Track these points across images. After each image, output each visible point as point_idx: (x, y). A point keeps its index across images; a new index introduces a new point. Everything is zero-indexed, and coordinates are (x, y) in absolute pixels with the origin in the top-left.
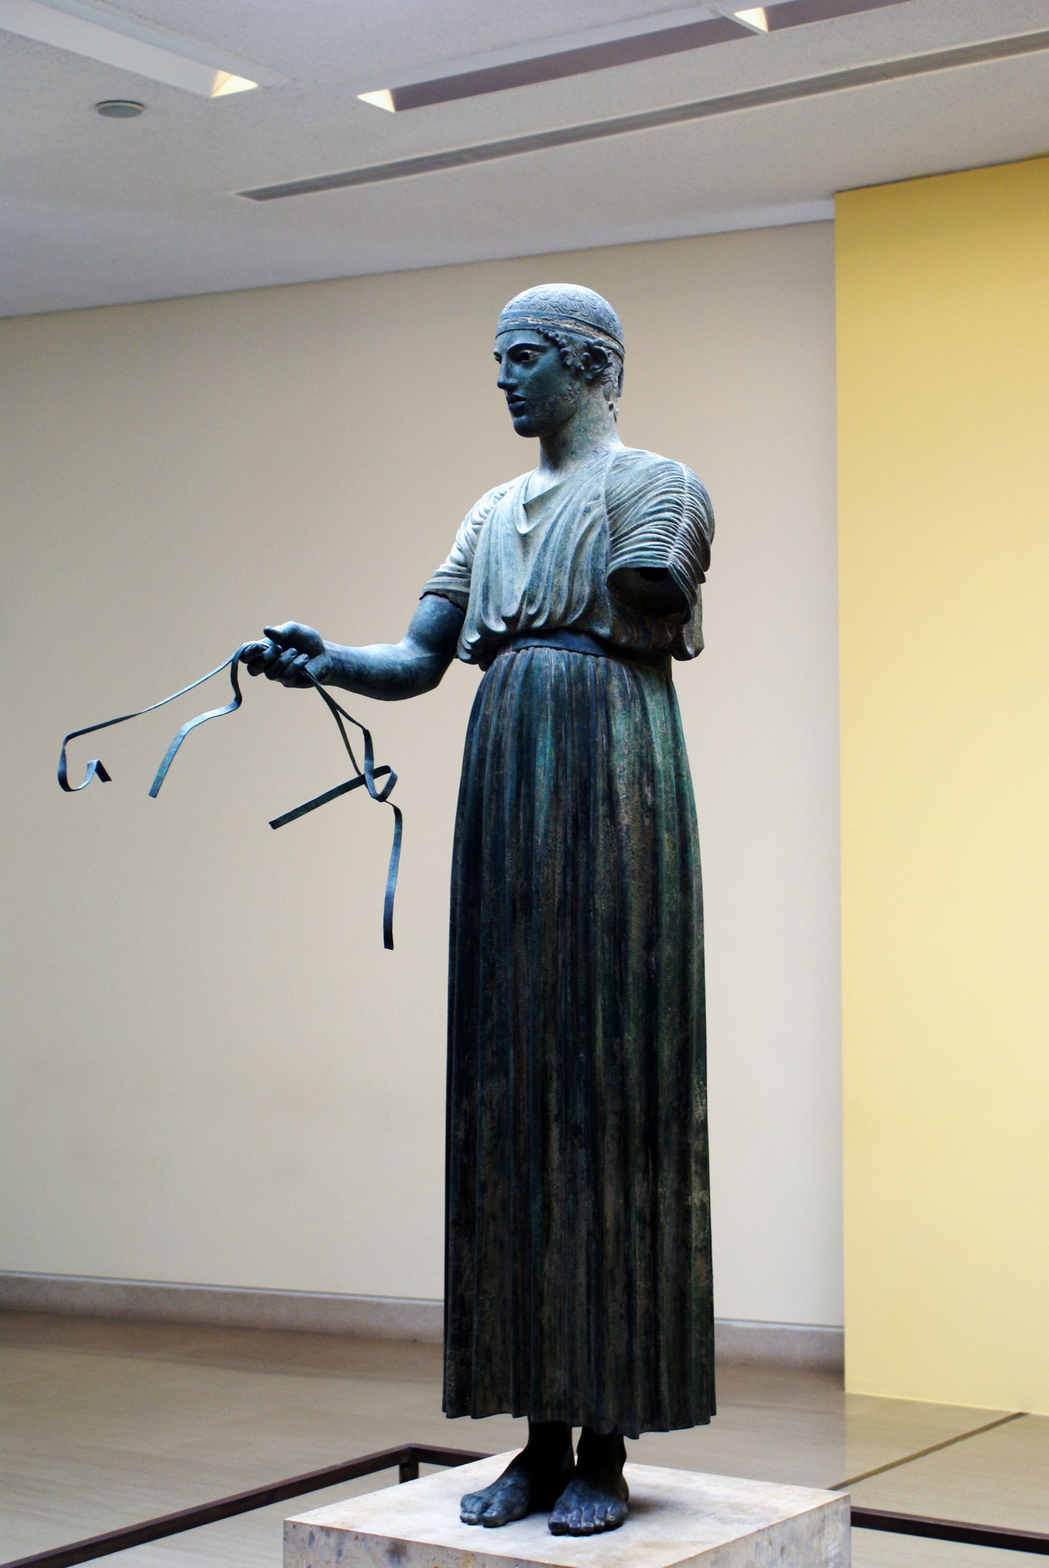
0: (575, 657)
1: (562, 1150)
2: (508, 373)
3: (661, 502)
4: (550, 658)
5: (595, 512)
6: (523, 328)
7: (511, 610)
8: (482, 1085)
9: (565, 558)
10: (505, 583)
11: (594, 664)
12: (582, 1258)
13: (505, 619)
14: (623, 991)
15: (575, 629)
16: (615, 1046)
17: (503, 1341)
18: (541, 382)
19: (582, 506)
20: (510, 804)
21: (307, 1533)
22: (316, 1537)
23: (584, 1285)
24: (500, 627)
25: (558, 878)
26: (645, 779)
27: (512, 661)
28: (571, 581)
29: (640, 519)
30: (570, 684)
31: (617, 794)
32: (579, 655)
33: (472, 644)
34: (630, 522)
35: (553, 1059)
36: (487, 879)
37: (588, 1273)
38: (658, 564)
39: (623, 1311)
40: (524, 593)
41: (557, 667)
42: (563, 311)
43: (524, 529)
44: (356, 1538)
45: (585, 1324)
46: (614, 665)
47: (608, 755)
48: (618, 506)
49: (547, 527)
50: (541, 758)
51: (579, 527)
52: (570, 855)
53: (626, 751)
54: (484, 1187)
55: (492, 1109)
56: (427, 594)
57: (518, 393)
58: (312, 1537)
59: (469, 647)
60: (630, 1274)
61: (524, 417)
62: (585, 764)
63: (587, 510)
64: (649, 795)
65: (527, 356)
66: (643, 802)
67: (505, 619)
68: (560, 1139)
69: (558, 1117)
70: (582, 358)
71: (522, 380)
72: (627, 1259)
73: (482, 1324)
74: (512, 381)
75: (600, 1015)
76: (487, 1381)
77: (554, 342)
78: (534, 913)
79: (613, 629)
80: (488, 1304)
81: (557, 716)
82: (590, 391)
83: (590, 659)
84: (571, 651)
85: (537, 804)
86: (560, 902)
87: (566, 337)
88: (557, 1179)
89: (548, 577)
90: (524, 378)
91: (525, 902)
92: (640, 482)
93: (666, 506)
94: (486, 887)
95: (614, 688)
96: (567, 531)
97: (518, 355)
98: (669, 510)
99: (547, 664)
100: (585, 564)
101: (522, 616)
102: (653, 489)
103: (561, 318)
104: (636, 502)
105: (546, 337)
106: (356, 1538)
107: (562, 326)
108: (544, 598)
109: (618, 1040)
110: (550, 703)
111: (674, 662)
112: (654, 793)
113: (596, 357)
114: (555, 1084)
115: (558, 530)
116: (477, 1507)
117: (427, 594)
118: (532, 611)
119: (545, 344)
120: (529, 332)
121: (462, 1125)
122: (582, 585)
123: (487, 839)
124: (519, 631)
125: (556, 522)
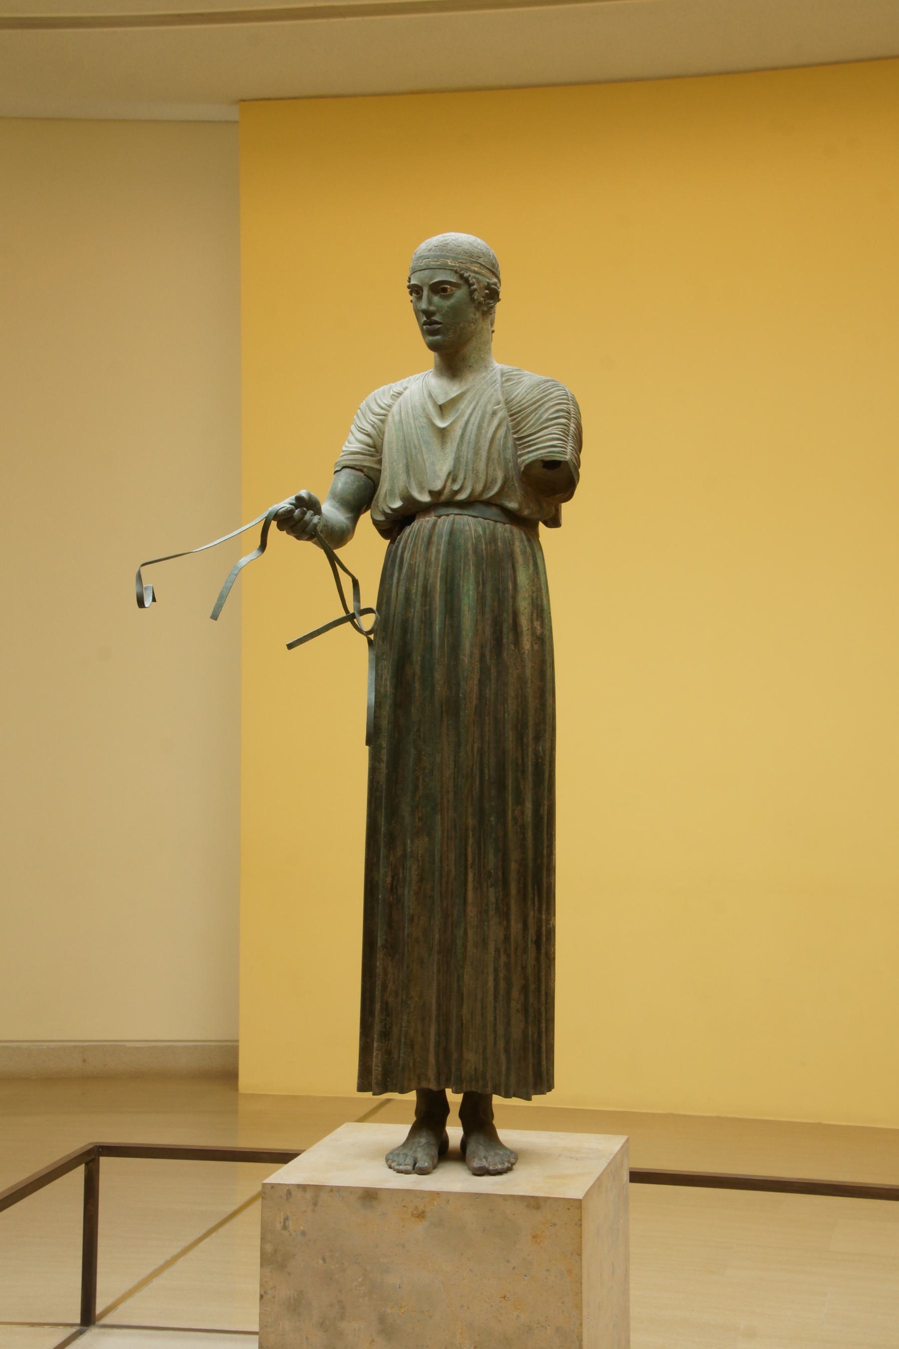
0: (489, 524)
1: (475, 889)
2: (430, 302)
3: (557, 411)
4: (470, 525)
5: (500, 414)
6: (444, 268)
7: (438, 486)
8: (412, 842)
9: (479, 449)
10: (428, 464)
11: (504, 530)
12: (491, 969)
13: (431, 493)
14: (524, 772)
15: (488, 503)
16: (516, 812)
17: (423, 1034)
18: (455, 311)
19: (489, 409)
20: (440, 632)
21: (285, 1191)
22: (293, 1193)
23: (492, 988)
24: (426, 498)
25: (476, 688)
26: (535, 615)
27: (435, 524)
28: (487, 465)
29: (541, 424)
30: (486, 545)
31: (521, 626)
32: (491, 522)
33: (391, 509)
34: (533, 425)
35: (471, 822)
36: (418, 688)
37: (496, 980)
38: (558, 457)
39: (519, 1006)
40: (449, 473)
41: (476, 531)
42: (472, 256)
43: (442, 425)
44: (332, 1190)
45: (492, 1018)
46: (516, 530)
47: (514, 598)
48: (520, 411)
49: (461, 423)
50: (466, 599)
51: (489, 426)
52: (484, 671)
53: (527, 595)
54: (412, 919)
55: (418, 860)
56: (344, 467)
57: (436, 318)
58: (289, 1193)
59: (389, 511)
60: (526, 978)
61: (438, 337)
62: (496, 604)
63: (494, 413)
64: (539, 628)
65: (445, 290)
66: (533, 633)
67: (431, 493)
68: (474, 881)
69: (473, 863)
70: (483, 294)
71: (439, 309)
72: (524, 968)
73: (409, 1022)
74: (432, 308)
75: (510, 788)
76: (411, 1064)
77: (466, 280)
78: (462, 714)
79: (520, 504)
80: (412, 1006)
81: (478, 567)
82: (483, 320)
83: (499, 525)
85: (464, 633)
86: (476, 707)
87: (475, 277)
88: (471, 911)
89: (467, 463)
91: (453, 707)
92: (535, 394)
93: (561, 414)
94: (417, 694)
95: (518, 548)
96: (480, 427)
97: (438, 289)
98: (563, 417)
99: (467, 528)
100: (495, 455)
101: (447, 491)
102: (549, 400)
103: (472, 262)
104: (536, 409)
105: (461, 277)
106: (332, 1190)
107: (473, 268)
108: (465, 478)
109: (519, 808)
110: (472, 558)
111: (541, 526)
112: (542, 626)
113: (493, 295)
114: (471, 841)
115: (470, 426)
116: (409, 1161)
117: (344, 467)
118: (456, 487)
119: (461, 282)
120: (449, 272)
121: (390, 873)
122: (495, 470)
123: (416, 657)
124: (442, 502)
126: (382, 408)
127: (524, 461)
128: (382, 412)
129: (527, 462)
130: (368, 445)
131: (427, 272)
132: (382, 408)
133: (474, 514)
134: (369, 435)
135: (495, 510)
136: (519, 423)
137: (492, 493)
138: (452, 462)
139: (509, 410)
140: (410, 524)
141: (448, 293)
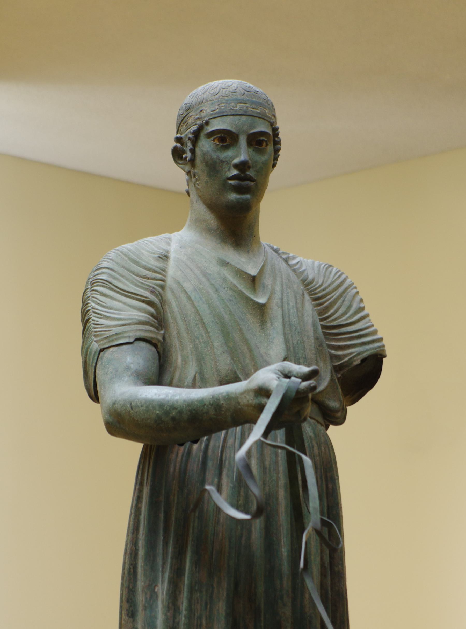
0: (314, 424)
43: (262, 300)
56: (138, 339)
65: (260, 143)
89: (294, 348)
104: (341, 296)
120: (267, 123)
125: (282, 299)
126: (155, 272)
127: (359, 354)
128: (159, 276)
129: (365, 355)
130: (152, 315)
131: (244, 118)
134: (150, 303)
136: (327, 309)
138: (283, 346)
139: (311, 293)
141: (262, 148)
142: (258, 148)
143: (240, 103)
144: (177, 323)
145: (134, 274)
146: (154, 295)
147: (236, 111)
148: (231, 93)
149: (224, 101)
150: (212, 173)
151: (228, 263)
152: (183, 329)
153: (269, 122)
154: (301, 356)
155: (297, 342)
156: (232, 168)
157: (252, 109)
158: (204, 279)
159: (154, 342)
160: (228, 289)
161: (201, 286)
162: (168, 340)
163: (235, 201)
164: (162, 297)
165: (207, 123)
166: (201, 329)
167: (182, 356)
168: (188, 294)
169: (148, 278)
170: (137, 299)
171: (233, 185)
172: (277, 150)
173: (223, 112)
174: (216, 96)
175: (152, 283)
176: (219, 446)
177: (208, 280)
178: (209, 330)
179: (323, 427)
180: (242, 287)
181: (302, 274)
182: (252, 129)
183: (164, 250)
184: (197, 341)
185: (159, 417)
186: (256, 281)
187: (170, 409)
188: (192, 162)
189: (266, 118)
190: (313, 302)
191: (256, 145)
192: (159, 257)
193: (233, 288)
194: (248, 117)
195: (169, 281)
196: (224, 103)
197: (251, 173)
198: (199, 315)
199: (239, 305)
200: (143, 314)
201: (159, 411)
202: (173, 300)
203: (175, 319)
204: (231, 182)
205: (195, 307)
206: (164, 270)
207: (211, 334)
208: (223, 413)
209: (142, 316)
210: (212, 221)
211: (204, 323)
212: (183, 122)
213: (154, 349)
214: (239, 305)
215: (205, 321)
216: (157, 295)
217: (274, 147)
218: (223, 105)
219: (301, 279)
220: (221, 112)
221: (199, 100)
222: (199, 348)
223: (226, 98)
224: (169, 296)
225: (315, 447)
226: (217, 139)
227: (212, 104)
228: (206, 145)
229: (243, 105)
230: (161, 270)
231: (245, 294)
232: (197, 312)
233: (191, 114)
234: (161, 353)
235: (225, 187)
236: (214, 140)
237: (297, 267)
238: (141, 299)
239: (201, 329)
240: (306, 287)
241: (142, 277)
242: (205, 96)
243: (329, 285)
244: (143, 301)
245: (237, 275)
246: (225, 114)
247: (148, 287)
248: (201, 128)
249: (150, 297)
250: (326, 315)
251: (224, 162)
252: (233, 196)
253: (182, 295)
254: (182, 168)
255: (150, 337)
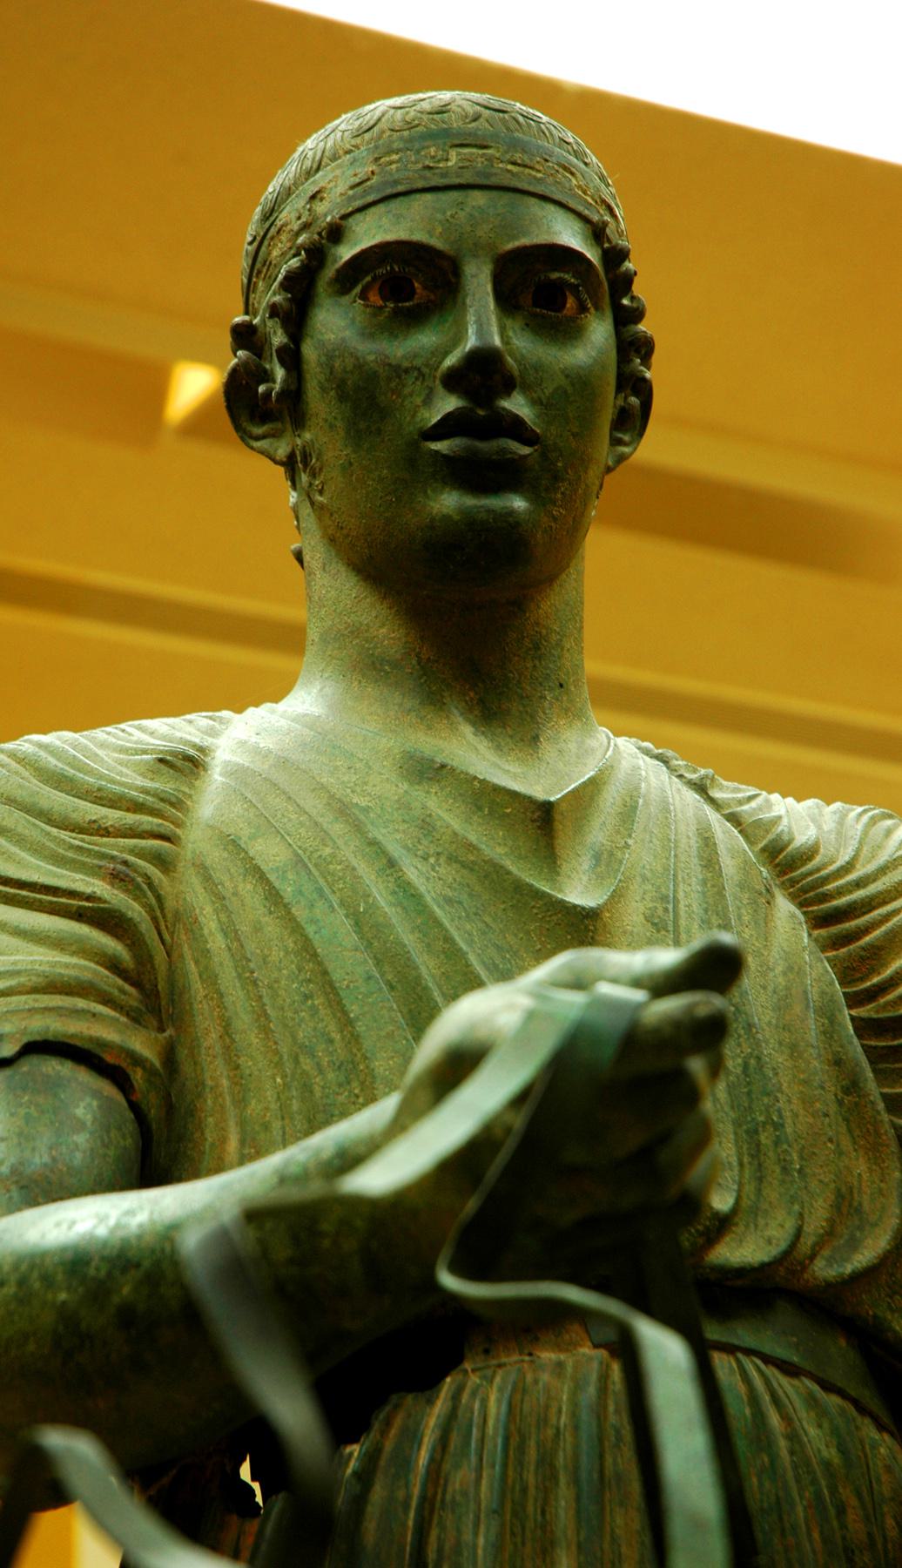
0: (843, 1412)
65: (551, 297)
84: (827, 1387)
90: (538, 367)
99: (774, 1419)
120: (577, 225)
128: (147, 821)
130: (114, 965)
131: (478, 199)
132: (136, 807)
133: (780, 1352)
135: (839, 1353)
136: (876, 955)
137: (863, 1257)
140: (427, 1383)
142: (543, 316)
143: (462, 146)
144: (221, 996)
145: (50, 822)
146: (127, 891)
147: (444, 175)
148: (425, 117)
149: (395, 146)
150: (362, 425)
151: (443, 766)
152: (243, 1020)
153: (585, 220)
154: (762, 1119)
155: (746, 1066)
156: (440, 390)
157: (510, 167)
158: (338, 829)
159: (109, 1058)
160: (442, 860)
161: (328, 851)
162: (186, 1068)
163: (457, 518)
164: (159, 898)
165: (336, 233)
166: (322, 1012)
167: (242, 1123)
168: (268, 881)
169: (105, 832)
170: (54, 910)
171: (444, 456)
172: (631, 343)
173: (396, 182)
174: (367, 136)
175: (123, 849)
176: (408, 1498)
177: (358, 828)
178: (354, 1010)
179: (886, 1437)
180: (497, 847)
181: (767, 832)
182: (515, 237)
183: (187, 743)
184: (307, 1064)
185: (67, 1317)
186: (558, 826)
187: (109, 1274)
188: (294, 396)
189: (572, 204)
190: (816, 933)
191: (536, 304)
192: (161, 760)
193: (461, 855)
194: (494, 194)
195: (196, 839)
196: (397, 151)
197: (517, 405)
198: (315, 955)
199: (488, 919)
200: (74, 960)
201: (69, 1289)
202: (208, 909)
203: (210, 979)
204: (440, 446)
205: (295, 927)
206: (178, 804)
207: (360, 1027)
208: (326, 1243)
209: (67, 966)
210: (384, 630)
211: (331, 984)
212: (258, 265)
213: (108, 1089)
214: (488, 919)
215: (337, 976)
216: (138, 887)
217: (618, 333)
218: (395, 157)
219: (761, 845)
220: (385, 183)
221: (308, 164)
222: (317, 1089)
223: (406, 133)
224: (190, 892)
225: (850, 1511)
226: (377, 286)
227: (355, 160)
228: (336, 323)
229: (474, 150)
230: (162, 800)
231: (509, 873)
232: (307, 950)
233: (279, 223)
234: (154, 1113)
235: (416, 467)
236: (363, 296)
237: (745, 807)
238: (68, 905)
239: (322, 1012)
240: (783, 873)
241: (82, 830)
242: (330, 143)
243: (883, 870)
244: (79, 916)
245: (480, 808)
246: (400, 188)
247: (102, 863)
248: (316, 256)
249: (106, 896)
250: (876, 980)
251: (407, 371)
252: (449, 502)
253: (248, 889)
254: (262, 452)
255: (91, 1039)
